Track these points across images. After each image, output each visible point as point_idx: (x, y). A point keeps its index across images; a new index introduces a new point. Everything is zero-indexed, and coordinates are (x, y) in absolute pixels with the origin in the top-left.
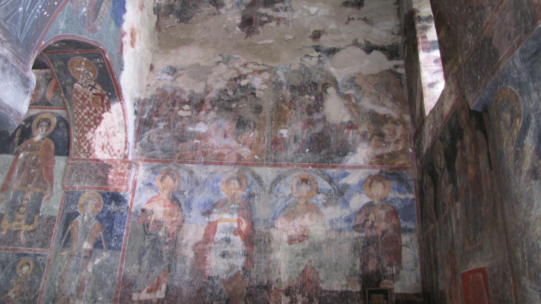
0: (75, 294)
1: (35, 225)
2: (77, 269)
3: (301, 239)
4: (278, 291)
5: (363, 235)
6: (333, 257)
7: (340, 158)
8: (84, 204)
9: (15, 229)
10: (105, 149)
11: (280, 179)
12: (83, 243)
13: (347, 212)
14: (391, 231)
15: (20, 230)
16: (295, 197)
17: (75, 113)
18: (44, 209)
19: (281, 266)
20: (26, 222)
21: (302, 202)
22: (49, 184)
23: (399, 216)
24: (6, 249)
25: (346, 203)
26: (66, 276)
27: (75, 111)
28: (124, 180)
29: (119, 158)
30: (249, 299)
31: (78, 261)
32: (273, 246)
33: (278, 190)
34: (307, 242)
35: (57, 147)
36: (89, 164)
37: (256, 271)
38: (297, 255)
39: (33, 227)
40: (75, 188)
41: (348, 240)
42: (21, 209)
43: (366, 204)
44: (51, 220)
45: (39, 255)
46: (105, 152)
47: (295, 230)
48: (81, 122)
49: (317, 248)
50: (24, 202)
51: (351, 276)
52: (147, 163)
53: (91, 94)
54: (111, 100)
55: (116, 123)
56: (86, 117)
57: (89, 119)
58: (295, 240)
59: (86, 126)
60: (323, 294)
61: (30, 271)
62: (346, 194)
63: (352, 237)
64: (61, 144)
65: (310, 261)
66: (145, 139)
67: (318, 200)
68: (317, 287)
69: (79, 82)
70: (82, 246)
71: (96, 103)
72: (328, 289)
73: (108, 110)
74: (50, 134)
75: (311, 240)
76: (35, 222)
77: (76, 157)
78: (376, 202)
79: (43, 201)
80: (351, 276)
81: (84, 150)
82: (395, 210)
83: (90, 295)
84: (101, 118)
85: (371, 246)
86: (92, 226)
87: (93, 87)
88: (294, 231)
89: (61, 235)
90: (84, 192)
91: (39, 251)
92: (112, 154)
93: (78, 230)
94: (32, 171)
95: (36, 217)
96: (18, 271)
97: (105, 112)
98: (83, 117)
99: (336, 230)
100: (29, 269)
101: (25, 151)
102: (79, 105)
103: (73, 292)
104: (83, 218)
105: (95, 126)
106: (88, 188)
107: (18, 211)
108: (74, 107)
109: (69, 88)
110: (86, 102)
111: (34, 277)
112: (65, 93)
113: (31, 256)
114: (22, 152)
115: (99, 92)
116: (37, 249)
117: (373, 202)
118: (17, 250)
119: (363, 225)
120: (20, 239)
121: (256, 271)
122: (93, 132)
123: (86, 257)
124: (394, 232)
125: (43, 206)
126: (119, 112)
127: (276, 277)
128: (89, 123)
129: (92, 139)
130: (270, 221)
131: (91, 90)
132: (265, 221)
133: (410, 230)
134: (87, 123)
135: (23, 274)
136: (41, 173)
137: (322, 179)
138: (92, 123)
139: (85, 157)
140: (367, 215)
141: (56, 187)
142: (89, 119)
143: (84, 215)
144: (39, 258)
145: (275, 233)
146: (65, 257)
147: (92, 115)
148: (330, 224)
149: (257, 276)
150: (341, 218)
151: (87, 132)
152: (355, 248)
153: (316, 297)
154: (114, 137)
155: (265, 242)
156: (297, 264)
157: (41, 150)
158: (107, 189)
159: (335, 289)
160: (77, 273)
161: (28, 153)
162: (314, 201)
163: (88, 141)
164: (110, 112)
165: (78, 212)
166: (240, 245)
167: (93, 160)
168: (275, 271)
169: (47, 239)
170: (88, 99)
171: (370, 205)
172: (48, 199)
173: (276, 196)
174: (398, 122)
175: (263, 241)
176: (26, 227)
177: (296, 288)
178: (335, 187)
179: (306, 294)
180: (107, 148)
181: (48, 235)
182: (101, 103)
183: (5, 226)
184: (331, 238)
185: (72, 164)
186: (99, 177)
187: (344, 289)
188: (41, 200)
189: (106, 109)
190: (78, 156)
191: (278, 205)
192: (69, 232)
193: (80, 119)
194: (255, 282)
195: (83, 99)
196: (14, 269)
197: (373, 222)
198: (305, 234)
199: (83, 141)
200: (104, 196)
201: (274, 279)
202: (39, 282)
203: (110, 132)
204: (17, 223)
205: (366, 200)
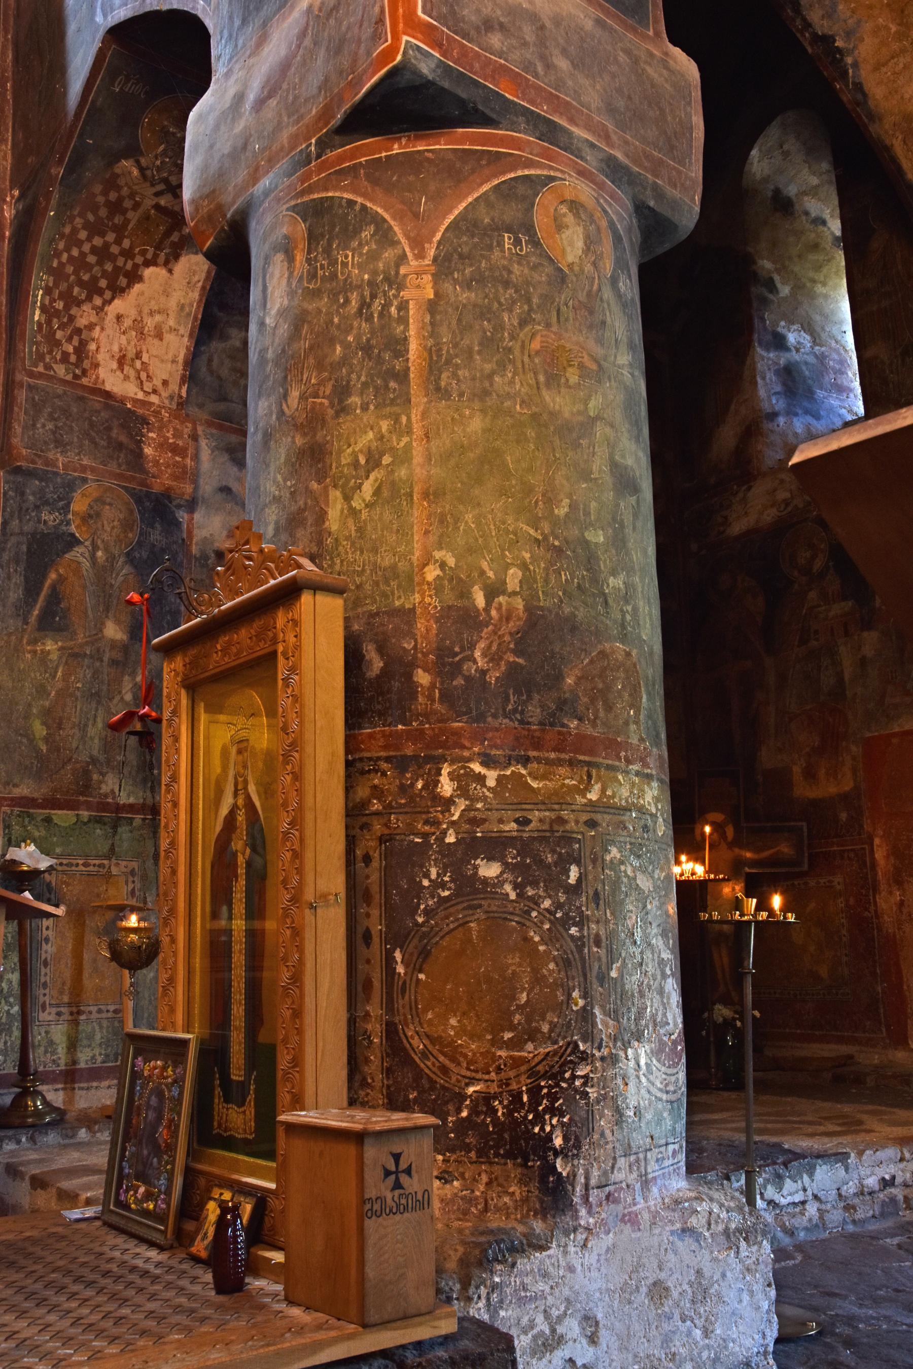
0: (102, 758)
2: (97, 694)
8: (90, 516)
10: (126, 368)
12: (103, 624)
17: (62, 236)
26: (68, 709)
27: (67, 230)
28: (185, 466)
29: (167, 402)
31: (96, 673)
36: (81, 399)
40: (54, 463)
46: (126, 378)
48: (70, 269)
52: (214, 431)
53: (149, 202)
55: (173, 304)
57: (96, 269)
59: (81, 283)
69: (143, 161)
70: (101, 631)
73: (166, 263)
77: (41, 369)
81: (66, 355)
83: (135, 763)
84: (134, 277)
86: (120, 579)
90: (85, 480)
92: (148, 387)
93: (84, 587)
97: (155, 264)
103: (95, 753)
104: (93, 556)
105: (108, 294)
106: (93, 470)
108: (72, 219)
110: (117, 220)
112: (69, 171)
122: (100, 310)
123: (114, 663)
126: (196, 278)
128: (95, 280)
129: (91, 327)
131: (158, 194)
134: (86, 277)
138: (103, 283)
139: (69, 377)
143: (95, 548)
146: (54, 656)
147: (113, 258)
151: (79, 304)
154: (156, 342)
158: (143, 483)
160: (99, 703)
163: (78, 331)
164: (170, 271)
165: (73, 535)
170: (130, 215)
180: (132, 366)
182: (157, 237)
185: (30, 388)
186: (120, 446)
189: (162, 257)
190: (48, 367)
192: (53, 587)
193: (71, 259)
199: (62, 327)
200: (139, 501)
203: (150, 323)
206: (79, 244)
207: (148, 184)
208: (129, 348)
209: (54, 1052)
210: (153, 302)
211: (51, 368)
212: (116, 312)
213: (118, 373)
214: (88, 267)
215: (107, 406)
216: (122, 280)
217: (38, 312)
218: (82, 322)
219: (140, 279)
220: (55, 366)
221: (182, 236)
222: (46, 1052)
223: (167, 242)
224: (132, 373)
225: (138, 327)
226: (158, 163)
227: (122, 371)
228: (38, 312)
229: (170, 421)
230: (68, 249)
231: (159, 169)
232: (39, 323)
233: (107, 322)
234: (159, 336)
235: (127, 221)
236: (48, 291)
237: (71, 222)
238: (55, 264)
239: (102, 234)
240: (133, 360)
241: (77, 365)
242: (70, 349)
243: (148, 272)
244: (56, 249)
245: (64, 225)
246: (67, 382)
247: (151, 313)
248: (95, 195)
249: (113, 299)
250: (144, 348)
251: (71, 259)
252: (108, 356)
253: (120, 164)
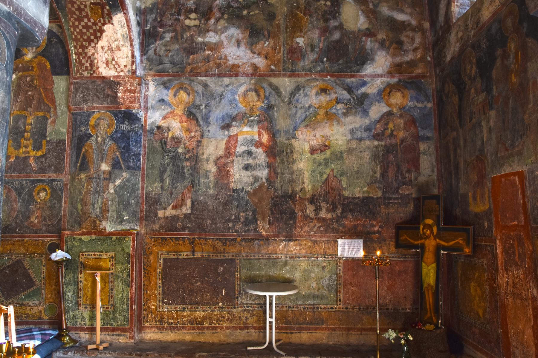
0: (100, 215)
1: (44, 151)
2: (99, 192)
3: (322, 149)
4: (303, 199)
5: (383, 143)
6: (354, 165)
7: (358, 67)
8: (96, 125)
9: (23, 156)
10: (110, 65)
11: (299, 90)
12: (100, 165)
13: (367, 121)
14: (409, 140)
15: (29, 157)
16: (315, 108)
17: (71, 26)
18: (51, 133)
19: (305, 176)
20: (34, 147)
21: (322, 112)
22: (51, 107)
23: (417, 125)
24: (18, 177)
25: (365, 113)
26: (88, 199)
27: (71, 24)
28: (135, 97)
29: (127, 73)
30: (275, 209)
31: (98, 184)
32: (295, 156)
33: (297, 101)
34: (328, 152)
35: (53, 66)
36: (94, 82)
37: (281, 182)
38: (320, 165)
39: (42, 152)
40: (83, 109)
41: (369, 148)
42: (26, 134)
43: (386, 113)
44: (61, 144)
45: (54, 180)
46: (110, 69)
47: (317, 139)
48: (79, 37)
49: (338, 156)
50: (27, 127)
51: (372, 183)
52: (157, 78)
54: (113, 10)
55: (119, 36)
56: (84, 30)
57: (88, 33)
58: (317, 150)
59: (85, 40)
60: (346, 200)
61: (48, 197)
62: (366, 103)
63: (372, 146)
64: (57, 63)
65: (332, 170)
66: (151, 52)
67: (337, 110)
68: (339, 195)
70: (100, 168)
71: (95, 14)
72: (351, 196)
73: (109, 22)
74: (42, 52)
75: (332, 149)
76: (43, 147)
77: (78, 75)
78: (395, 110)
79: (48, 125)
80: (372, 183)
81: (87, 67)
82: (413, 118)
83: (115, 216)
84: (102, 31)
85: (390, 154)
86: (108, 147)
88: (315, 141)
89: (74, 159)
90: (94, 112)
91: (54, 176)
92: (119, 70)
93: (93, 152)
94: (30, 93)
95: (44, 142)
96: (35, 197)
99: (356, 139)
100: (47, 195)
101: (17, 72)
103: (98, 214)
104: (97, 140)
105: (95, 41)
106: (97, 108)
107: (23, 136)
108: (70, 19)
110: (84, 13)
111: (53, 202)
113: (46, 182)
114: (13, 73)
116: (51, 174)
117: (392, 111)
118: (30, 176)
119: (383, 134)
120: (31, 165)
121: (281, 182)
122: (95, 47)
123: (105, 179)
124: (412, 140)
125: (49, 129)
126: (123, 24)
127: (300, 187)
128: (89, 37)
129: (93, 54)
130: (291, 131)
132: (286, 132)
133: (428, 138)
134: (86, 37)
135: (41, 200)
136: (40, 94)
137: (341, 89)
138: (92, 37)
139: (89, 75)
140: (387, 124)
141: (60, 109)
142: (88, 33)
143: (97, 137)
144: (55, 183)
145: (296, 144)
146: (84, 180)
147: (91, 27)
148: (351, 133)
149: (282, 186)
150: (361, 127)
151: (87, 47)
152: (375, 156)
153: (339, 203)
154: (118, 52)
155: (287, 153)
156: (320, 173)
157: (35, 70)
158: (118, 108)
159: (358, 196)
160: (99, 195)
161: (20, 74)
162: (334, 111)
163: (89, 57)
164: (112, 24)
165: (90, 134)
166: (263, 157)
167: (98, 78)
168: (299, 181)
169: (59, 163)
170: (86, 10)
171: (389, 114)
172: (54, 122)
173: (296, 107)
174: (417, 29)
175: (285, 152)
176: (34, 152)
177: (320, 196)
178: (354, 96)
179: (330, 201)
180: (112, 64)
181: (60, 159)
183: (12, 153)
184: (352, 147)
185: (75, 83)
186: (108, 96)
187: (366, 195)
188: (46, 124)
190: (81, 74)
191: (299, 115)
192: (84, 154)
194: (280, 192)
195: (80, 9)
196: (31, 195)
197: (392, 131)
198: (327, 144)
199: (84, 58)
200: (115, 115)
201: (298, 189)
202: (61, 206)
203: (114, 45)
204: (24, 149)
205: (385, 109)
206: (77, 27)
209: (84, 321)
210: (112, 38)
211: (82, 74)
213: (107, 68)
215: (103, 82)
216: (98, 34)
217: (74, 55)
218: (90, 54)
221: (108, 10)
222: (81, 320)
223: (105, 15)
224: (112, 67)
228: (74, 55)
229: (129, 81)
232: (76, 60)
234: (119, 49)
235: (87, 13)
237: (70, 20)
238: (74, 37)
240: (111, 62)
241: (91, 70)
243: (105, 27)
244: (71, 32)
247: (113, 42)
250: (115, 56)
251: (77, 33)
252: (102, 63)
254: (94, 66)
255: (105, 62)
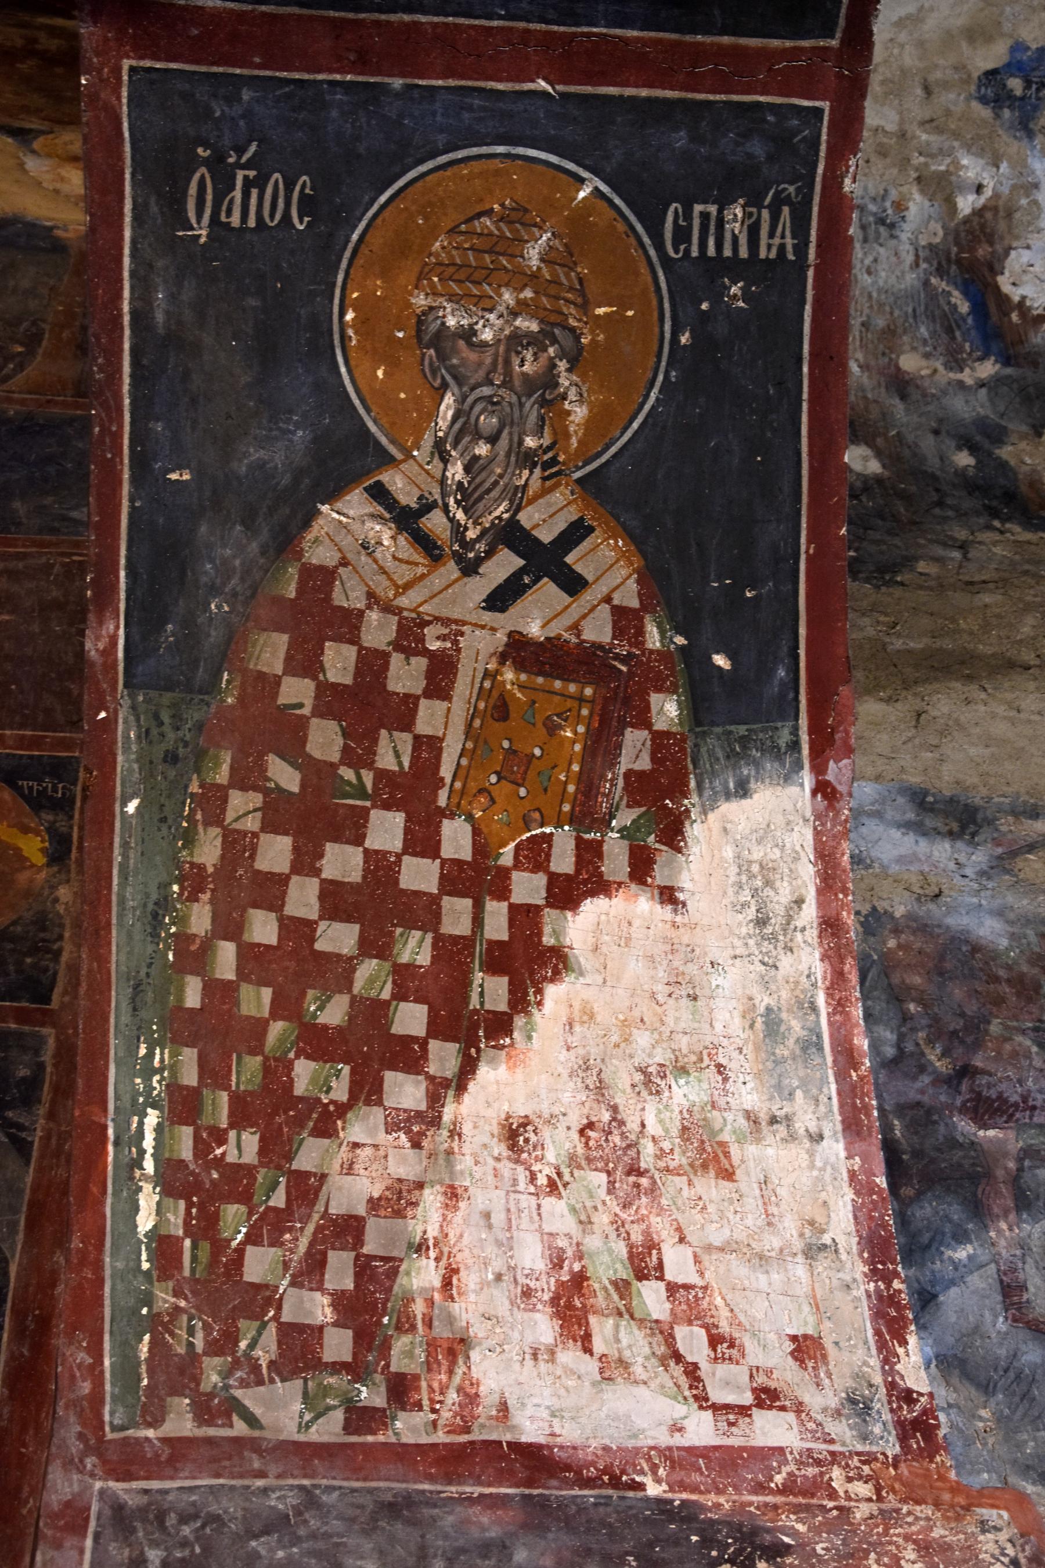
10: (602, 1329)
17: (195, 881)
27: (209, 851)
29: (842, 1431)
36: (397, 1508)
46: (613, 1369)
48: (257, 1001)
53: (480, 646)
55: (727, 1021)
59: (318, 1043)
66: (969, 1300)
71: (516, 767)
73: (641, 868)
77: (180, 1421)
84: (530, 962)
87: (547, 563)
92: (727, 1384)
97: (602, 887)
98: (299, 931)
102: (285, 776)
105: (444, 1058)
108: (213, 802)
109: (226, 550)
110: (392, 753)
112: (146, 618)
115: (598, 630)
122: (420, 1125)
126: (782, 896)
128: (372, 1013)
129: (398, 1200)
131: (500, 599)
134: (334, 1013)
138: (411, 1019)
139: (329, 1429)
142: (367, 969)
147: (423, 912)
151: (327, 1122)
154: (709, 1187)
163: (347, 1230)
164: (668, 896)
167: (457, 1459)
170: (429, 718)
180: (628, 1312)
182: (567, 777)
185: (121, 1519)
189: (616, 858)
193: (253, 959)
195: (368, 706)
199: (270, 1228)
203: (655, 1120)
206: (270, 891)
207: (451, 570)
208: (593, 1242)
210: (642, 1039)
212: (494, 1115)
213: (570, 1356)
214: (336, 972)
215: (539, 1515)
216: (487, 987)
217: (148, 1199)
218: (351, 1192)
219: (557, 962)
220: (249, 1398)
223: (614, 785)
224: (636, 1345)
225: (613, 1153)
226: (456, 472)
227: (586, 1345)
228: (148, 1199)
229: (888, 1518)
230: (229, 927)
231: (469, 498)
232: (164, 1246)
233: (464, 1163)
234: (715, 1161)
235: (428, 748)
236: (183, 1106)
237: (215, 818)
238: (193, 996)
239: (352, 829)
240: (622, 1287)
241: (356, 1370)
242: (319, 1309)
243: (580, 928)
244: (183, 939)
245: (189, 839)
246: (324, 1451)
247: (650, 1081)
248: (271, 684)
249: (468, 1068)
250: (662, 1228)
251: (253, 959)
252: (500, 1300)
253: (319, 528)
254: (405, 1324)
255: (546, 1287)
